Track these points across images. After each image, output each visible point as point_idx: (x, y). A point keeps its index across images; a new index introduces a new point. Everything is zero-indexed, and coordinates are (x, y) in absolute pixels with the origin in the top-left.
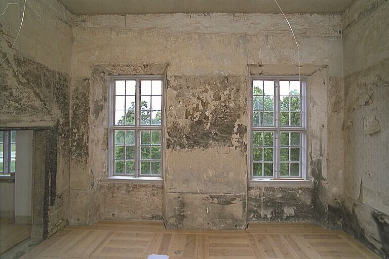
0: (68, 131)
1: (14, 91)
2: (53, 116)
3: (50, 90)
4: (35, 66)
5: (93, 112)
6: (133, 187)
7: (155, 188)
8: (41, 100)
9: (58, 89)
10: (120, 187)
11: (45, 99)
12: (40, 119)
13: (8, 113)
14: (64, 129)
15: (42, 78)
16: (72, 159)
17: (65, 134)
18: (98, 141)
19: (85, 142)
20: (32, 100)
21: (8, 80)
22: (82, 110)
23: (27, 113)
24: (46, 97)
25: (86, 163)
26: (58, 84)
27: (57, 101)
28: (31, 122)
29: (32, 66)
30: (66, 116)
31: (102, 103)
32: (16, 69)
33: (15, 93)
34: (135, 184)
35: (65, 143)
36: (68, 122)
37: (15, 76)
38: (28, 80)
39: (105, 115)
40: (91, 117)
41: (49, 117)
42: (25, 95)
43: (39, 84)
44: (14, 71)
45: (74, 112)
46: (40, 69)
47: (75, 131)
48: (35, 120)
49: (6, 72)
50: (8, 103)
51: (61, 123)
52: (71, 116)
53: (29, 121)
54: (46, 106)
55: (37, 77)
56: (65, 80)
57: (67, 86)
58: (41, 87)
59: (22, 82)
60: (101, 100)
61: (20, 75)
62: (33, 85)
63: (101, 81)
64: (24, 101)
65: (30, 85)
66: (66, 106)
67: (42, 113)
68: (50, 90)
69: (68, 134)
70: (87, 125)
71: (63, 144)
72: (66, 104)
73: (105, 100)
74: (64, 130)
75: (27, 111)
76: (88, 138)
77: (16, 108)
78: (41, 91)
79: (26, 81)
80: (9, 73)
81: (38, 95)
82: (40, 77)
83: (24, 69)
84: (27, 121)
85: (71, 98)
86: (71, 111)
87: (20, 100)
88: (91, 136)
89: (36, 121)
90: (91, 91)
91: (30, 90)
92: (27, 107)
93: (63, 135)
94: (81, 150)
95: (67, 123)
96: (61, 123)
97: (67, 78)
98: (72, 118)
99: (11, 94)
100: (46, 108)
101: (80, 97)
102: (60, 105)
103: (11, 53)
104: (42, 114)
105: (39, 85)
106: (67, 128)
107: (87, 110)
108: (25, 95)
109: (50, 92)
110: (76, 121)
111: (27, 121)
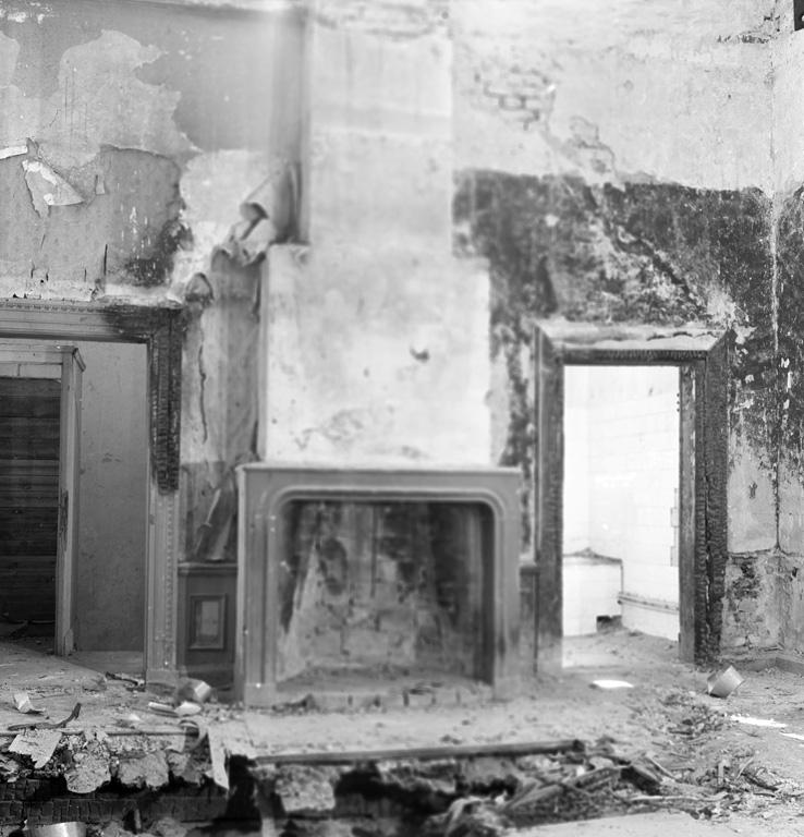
8: (675, 281)
11: (687, 277)
15: (675, 223)
28: (649, 339)
36: (769, 338)
41: (702, 324)
44: (607, 223)
49: (593, 228)
51: (740, 340)
54: (691, 296)
55: (663, 222)
59: (624, 244)
62: (651, 245)
64: (633, 288)
65: (645, 245)
72: (760, 281)
79: (633, 238)
80: (597, 228)
81: (663, 268)
91: (645, 259)
92: (640, 300)
96: (740, 340)
99: (603, 274)
100: (690, 300)
105: (664, 244)
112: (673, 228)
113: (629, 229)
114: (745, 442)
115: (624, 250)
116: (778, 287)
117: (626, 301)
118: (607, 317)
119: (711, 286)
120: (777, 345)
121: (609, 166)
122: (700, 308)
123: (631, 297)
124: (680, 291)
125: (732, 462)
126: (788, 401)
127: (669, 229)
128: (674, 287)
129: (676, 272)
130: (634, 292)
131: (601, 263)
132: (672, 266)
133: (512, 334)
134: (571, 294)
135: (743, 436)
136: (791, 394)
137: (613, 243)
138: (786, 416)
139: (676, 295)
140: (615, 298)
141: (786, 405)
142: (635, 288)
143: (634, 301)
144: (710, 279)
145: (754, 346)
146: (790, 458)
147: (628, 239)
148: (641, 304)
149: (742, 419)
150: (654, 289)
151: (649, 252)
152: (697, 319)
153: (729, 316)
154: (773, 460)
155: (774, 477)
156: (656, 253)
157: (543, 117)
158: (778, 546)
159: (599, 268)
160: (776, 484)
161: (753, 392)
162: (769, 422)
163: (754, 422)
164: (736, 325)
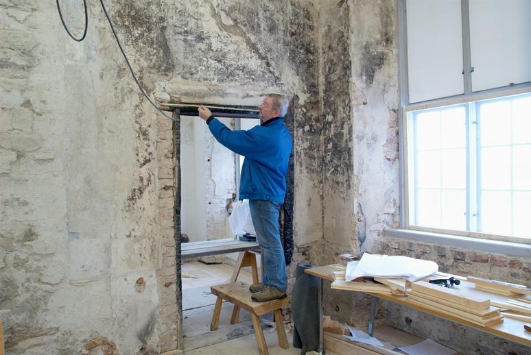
0: (317, 120)
1: (214, 41)
2: (285, 88)
3: (277, 37)
5: (359, 71)
6: (456, 259)
7: (520, 272)
8: (261, 57)
9: (293, 34)
11: (268, 55)
12: (261, 93)
13: (206, 79)
14: (309, 114)
15: (260, 16)
16: (326, 179)
17: (311, 126)
18: (375, 139)
19: (347, 141)
21: (204, 23)
22: (339, 71)
23: (236, 80)
24: (270, 50)
25: (349, 186)
26: (292, 23)
27: (292, 59)
30: (312, 88)
31: (380, 49)
33: (216, 45)
34: (460, 249)
35: (311, 144)
36: (317, 102)
37: (215, 15)
38: (235, 20)
39: (390, 77)
40: (357, 83)
44: (212, 7)
45: (326, 79)
47: (330, 118)
48: (250, 94)
49: (201, 10)
50: (205, 63)
51: (301, 102)
52: (322, 88)
53: (241, 95)
54: (271, 69)
55: (252, 14)
56: (308, 16)
57: (311, 28)
58: (260, 32)
59: (225, 25)
60: (378, 43)
61: (223, 14)
62: (244, 29)
64: (231, 59)
65: (240, 28)
67: (263, 81)
68: (277, 37)
69: (317, 128)
70: (347, 103)
71: (306, 145)
72: (311, 64)
74: (310, 119)
75: (236, 77)
76: (350, 132)
77: (218, 72)
79: (232, 23)
81: (253, 47)
82: (257, 15)
84: (237, 96)
85: (320, 51)
86: (322, 79)
87: (224, 56)
88: (357, 127)
89: (251, 96)
90: (353, 23)
92: (237, 69)
93: (307, 128)
94: (340, 158)
95: (314, 104)
96: (301, 102)
97: (312, 11)
98: (325, 91)
99: (210, 46)
100: (270, 72)
101: (334, 45)
102: (298, 67)
104: (262, 83)
105: (255, 29)
106: (315, 114)
107: (347, 68)
108: (232, 47)
109: (278, 41)
110: (331, 97)
112: (259, 20)
114: (305, 171)
115: (226, 30)
116: (324, 68)
117: (227, 68)
118: (214, 79)
119: (284, 64)
120: (323, 106)
123: (231, 65)
124: (265, 65)
125: (297, 185)
126: (331, 144)
130: (233, 62)
131: (208, 38)
134: (186, 58)
135: (304, 167)
136: (333, 138)
137: (217, 23)
138: (330, 153)
141: (330, 146)
142: (233, 59)
143: (233, 69)
144: (283, 59)
145: (309, 107)
146: (333, 181)
149: (303, 155)
150: (247, 61)
151: (243, 34)
152: (275, 86)
153: (295, 85)
154: (321, 182)
155: (321, 193)
156: (248, 35)
158: (323, 237)
159: (207, 41)
160: (322, 197)
161: (309, 137)
162: (318, 157)
163: (310, 157)
164: (299, 91)
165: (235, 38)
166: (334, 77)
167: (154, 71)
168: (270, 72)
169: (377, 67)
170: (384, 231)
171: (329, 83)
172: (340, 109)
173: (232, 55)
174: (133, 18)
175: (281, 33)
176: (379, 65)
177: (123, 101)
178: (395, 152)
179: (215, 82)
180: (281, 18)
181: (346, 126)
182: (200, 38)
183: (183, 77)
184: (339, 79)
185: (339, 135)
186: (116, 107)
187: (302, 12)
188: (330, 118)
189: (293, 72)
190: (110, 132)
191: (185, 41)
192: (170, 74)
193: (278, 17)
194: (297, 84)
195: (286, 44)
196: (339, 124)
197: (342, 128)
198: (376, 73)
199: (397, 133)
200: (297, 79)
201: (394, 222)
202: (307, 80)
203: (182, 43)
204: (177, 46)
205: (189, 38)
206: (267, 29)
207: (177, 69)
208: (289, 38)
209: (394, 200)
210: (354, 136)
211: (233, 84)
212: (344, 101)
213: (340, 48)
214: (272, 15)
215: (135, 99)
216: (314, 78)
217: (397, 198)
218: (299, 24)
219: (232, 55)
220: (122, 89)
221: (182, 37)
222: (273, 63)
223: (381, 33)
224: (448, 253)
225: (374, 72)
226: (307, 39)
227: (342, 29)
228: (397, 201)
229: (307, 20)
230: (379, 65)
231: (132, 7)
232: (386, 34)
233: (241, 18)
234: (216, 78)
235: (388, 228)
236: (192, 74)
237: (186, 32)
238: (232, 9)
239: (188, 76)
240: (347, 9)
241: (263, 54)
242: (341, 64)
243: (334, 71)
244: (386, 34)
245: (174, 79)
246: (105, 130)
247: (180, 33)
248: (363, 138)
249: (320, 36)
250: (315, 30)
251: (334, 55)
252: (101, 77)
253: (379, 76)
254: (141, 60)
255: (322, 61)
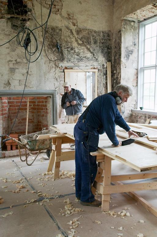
2: (99, 62)
4: (87, 32)
8: (91, 53)
9: (102, 43)
10: (141, 116)
11: (94, 52)
12: (91, 65)
18: (129, 79)
20: (86, 53)
26: (102, 39)
27: (102, 52)
28: (85, 67)
29: (85, 33)
31: (132, 48)
32: (76, 37)
33: (77, 50)
34: (150, 114)
37: (76, 41)
38: (83, 42)
42: (82, 51)
43: (90, 43)
44: (76, 38)
45: (114, 58)
46: (90, 33)
49: (72, 40)
53: (85, 66)
54: (95, 56)
55: (88, 38)
56: (108, 36)
57: (110, 40)
60: (131, 46)
61: (79, 40)
62: (86, 44)
63: (131, 30)
65: (84, 44)
66: (109, 55)
73: (135, 45)
75: (83, 60)
77: (78, 59)
78: (91, 47)
79: (82, 42)
80: (73, 40)
81: (89, 50)
82: (90, 38)
83: (81, 36)
84: (83, 66)
85: (113, 48)
86: (113, 58)
87: (79, 54)
89: (88, 66)
92: (84, 57)
97: (110, 33)
98: (114, 62)
99: (75, 51)
102: (104, 54)
103: (74, 28)
105: (89, 43)
107: (120, 55)
108: (82, 51)
109: (97, 46)
111: (83, 66)
112: (91, 40)
113: (80, 40)
115: (80, 45)
116: (114, 54)
121: (76, 24)
122: (97, 59)
123: (81, 57)
124: (92, 55)
127: (90, 40)
128: (91, 54)
129: (92, 51)
131: (74, 48)
132: (91, 49)
133: (54, 66)
137: (77, 43)
139: (91, 56)
140: (78, 57)
141: (115, 81)
142: (82, 54)
147: (80, 42)
148: (83, 58)
151: (85, 46)
153: (103, 61)
156: (87, 46)
157: (60, 10)
164: (105, 63)
165: (83, 47)
166: (116, 58)
167: (59, 61)
168: (94, 57)
169: (130, 55)
170: (131, 110)
171: (115, 60)
172: (118, 69)
173: (82, 53)
174: (53, 45)
175: (98, 43)
176: (131, 54)
177: (51, 70)
178: (136, 83)
179: (76, 62)
180: (99, 38)
181: (119, 75)
182: (72, 49)
183: (67, 62)
184: (118, 59)
185: (117, 78)
186: (49, 72)
187: (106, 35)
188: (115, 72)
189: (102, 56)
190: (47, 79)
191: (68, 50)
192: (63, 61)
193: (98, 38)
194: (104, 61)
195: (100, 47)
196: (117, 74)
197: (118, 76)
198: (130, 57)
199: (137, 77)
200: (104, 59)
201: (135, 107)
202: (107, 58)
203: (67, 51)
204: (65, 52)
205: (69, 49)
206: (93, 42)
207: (65, 59)
208: (101, 45)
209: (135, 100)
210: (121, 78)
211: (82, 62)
212: (119, 66)
213: (118, 48)
214: (95, 37)
215: (54, 69)
216: (110, 58)
217: (136, 99)
218: (105, 39)
219: (82, 53)
220: (50, 67)
221: (67, 49)
222: (95, 54)
223: (133, 42)
224: (147, 116)
225: (129, 56)
226: (108, 44)
227: (119, 41)
228: (136, 100)
229: (108, 37)
230: (131, 54)
231: (52, 42)
232: (134, 43)
233: (85, 40)
234: (77, 61)
235: (133, 109)
236: (70, 61)
237: (68, 48)
238: (82, 38)
239: (68, 61)
240: (121, 34)
241: (92, 52)
242: (118, 54)
243: (117, 56)
244: (134, 43)
245: (64, 63)
246: (46, 79)
247: (66, 48)
248: (124, 79)
249: (113, 43)
250: (111, 40)
251: (117, 50)
252: (45, 64)
253: (131, 57)
254: (55, 58)
255: (113, 51)
